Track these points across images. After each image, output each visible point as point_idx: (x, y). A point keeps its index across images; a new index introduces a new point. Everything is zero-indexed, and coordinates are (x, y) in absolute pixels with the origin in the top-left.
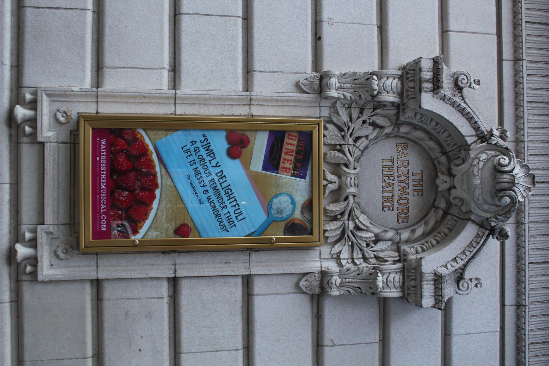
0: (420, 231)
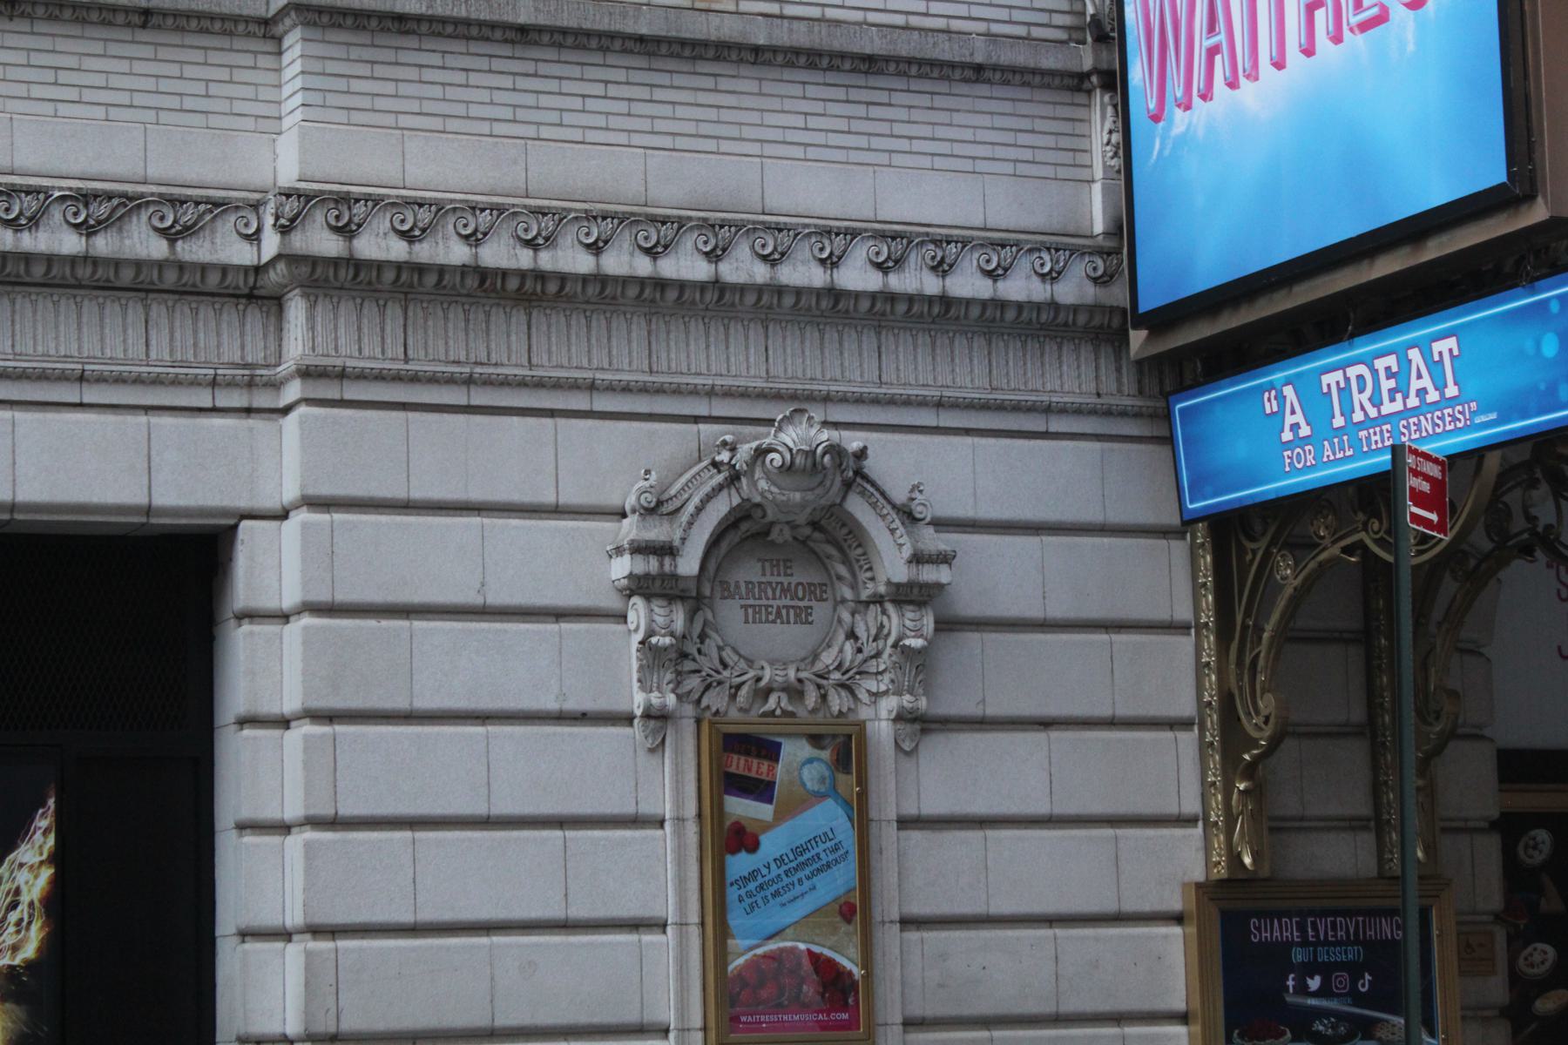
0: (842, 570)
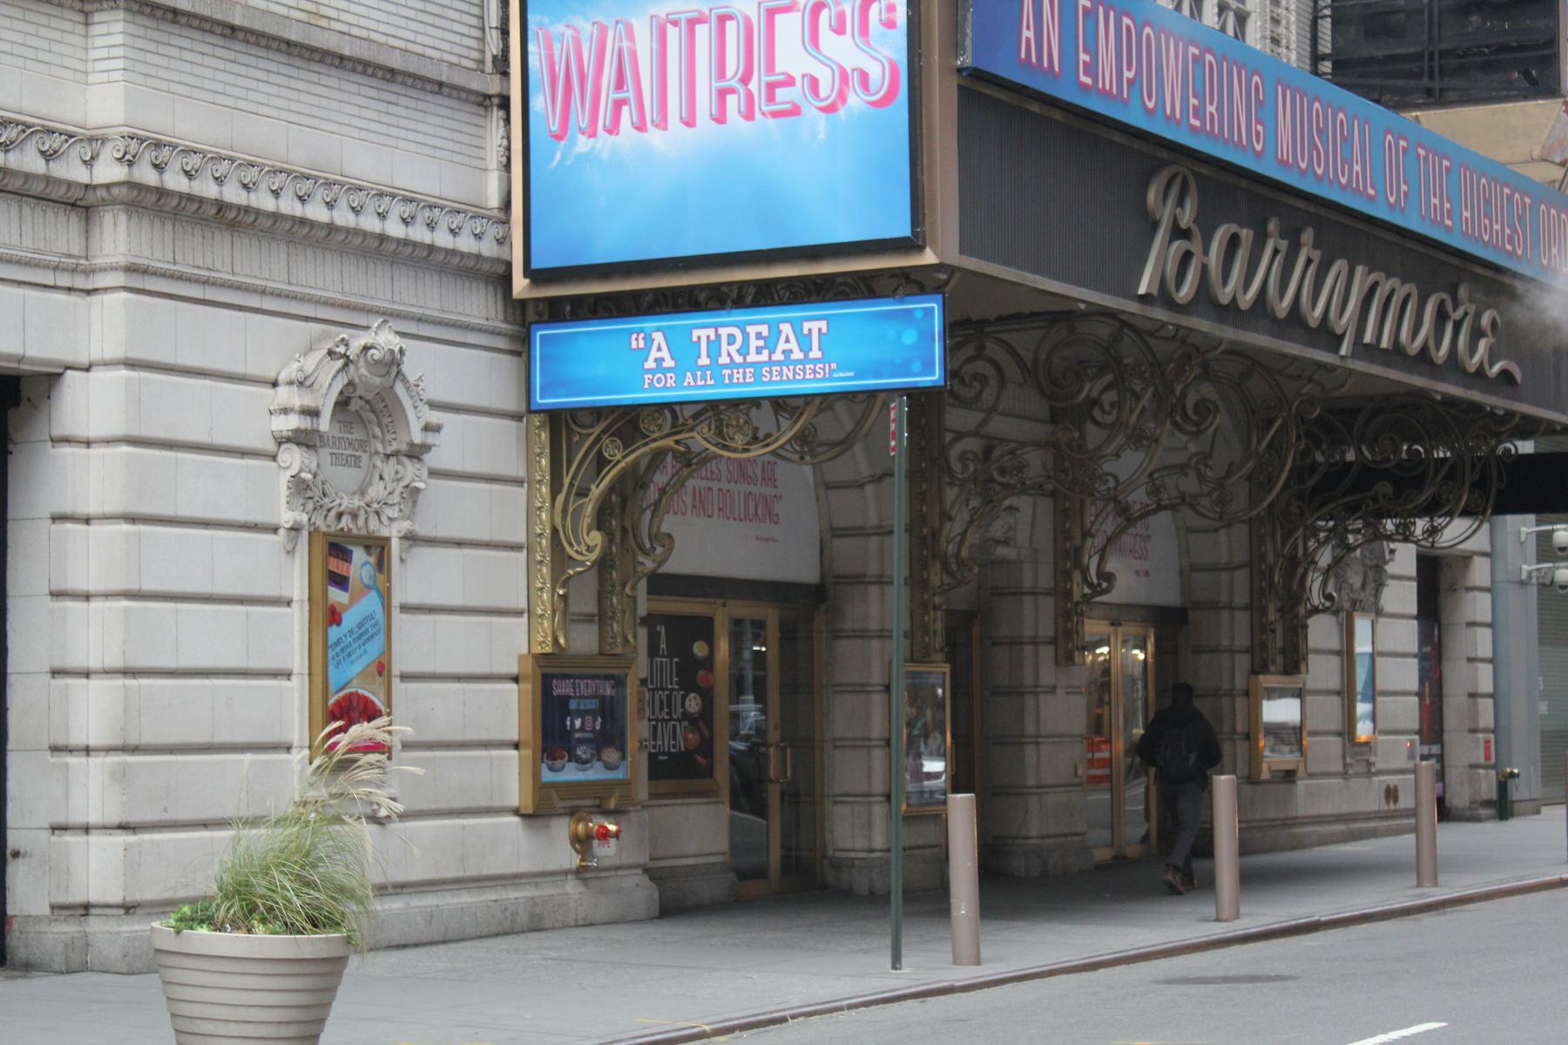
0: (378, 431)
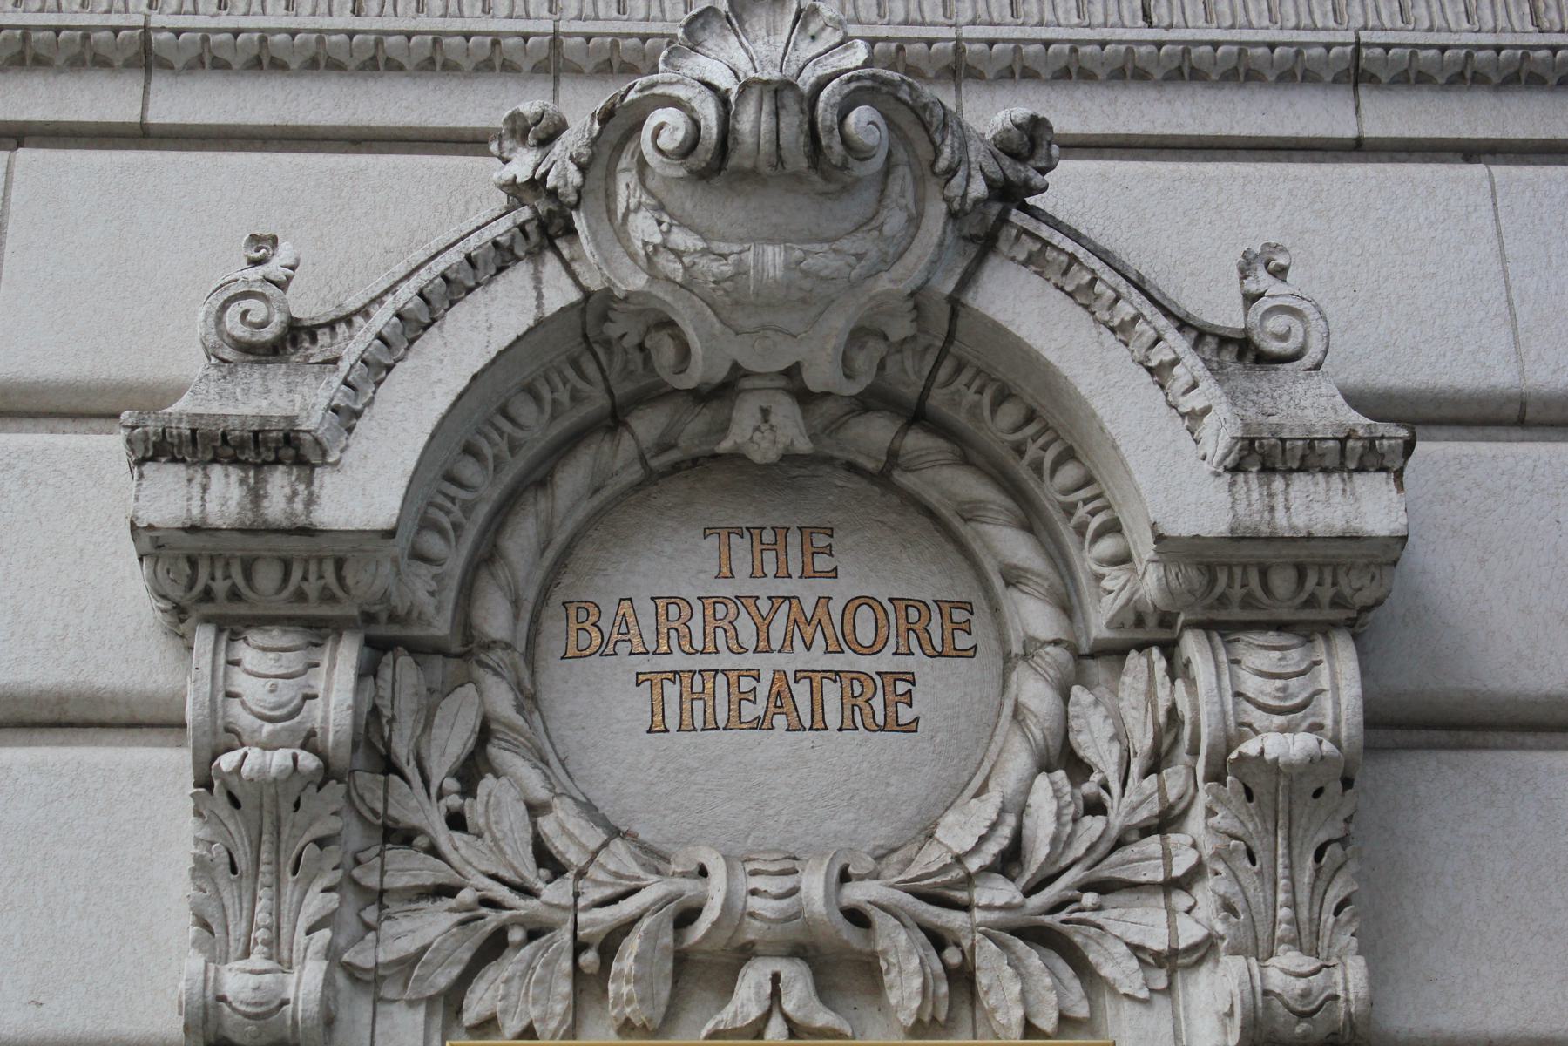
0: (1016, 547)
